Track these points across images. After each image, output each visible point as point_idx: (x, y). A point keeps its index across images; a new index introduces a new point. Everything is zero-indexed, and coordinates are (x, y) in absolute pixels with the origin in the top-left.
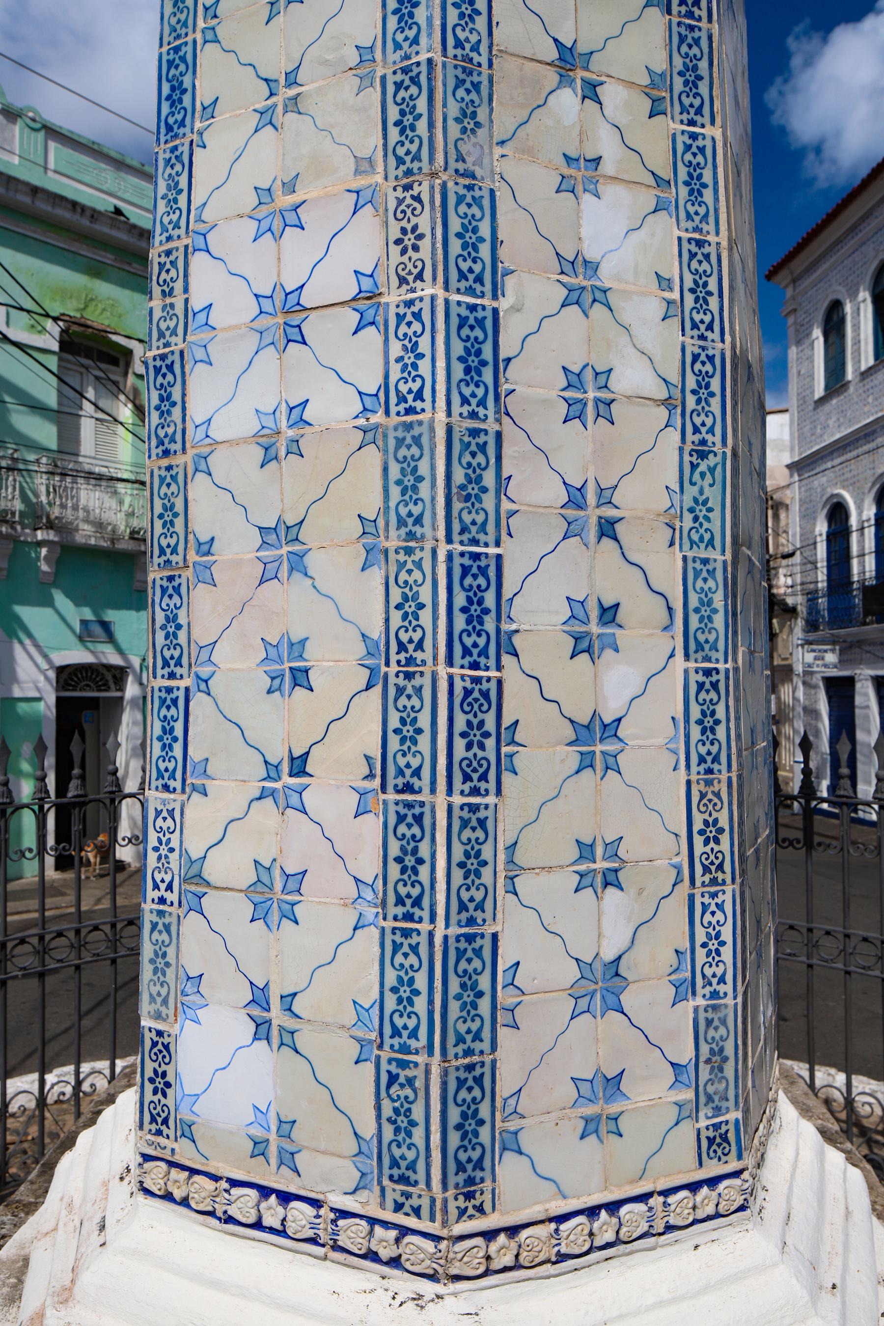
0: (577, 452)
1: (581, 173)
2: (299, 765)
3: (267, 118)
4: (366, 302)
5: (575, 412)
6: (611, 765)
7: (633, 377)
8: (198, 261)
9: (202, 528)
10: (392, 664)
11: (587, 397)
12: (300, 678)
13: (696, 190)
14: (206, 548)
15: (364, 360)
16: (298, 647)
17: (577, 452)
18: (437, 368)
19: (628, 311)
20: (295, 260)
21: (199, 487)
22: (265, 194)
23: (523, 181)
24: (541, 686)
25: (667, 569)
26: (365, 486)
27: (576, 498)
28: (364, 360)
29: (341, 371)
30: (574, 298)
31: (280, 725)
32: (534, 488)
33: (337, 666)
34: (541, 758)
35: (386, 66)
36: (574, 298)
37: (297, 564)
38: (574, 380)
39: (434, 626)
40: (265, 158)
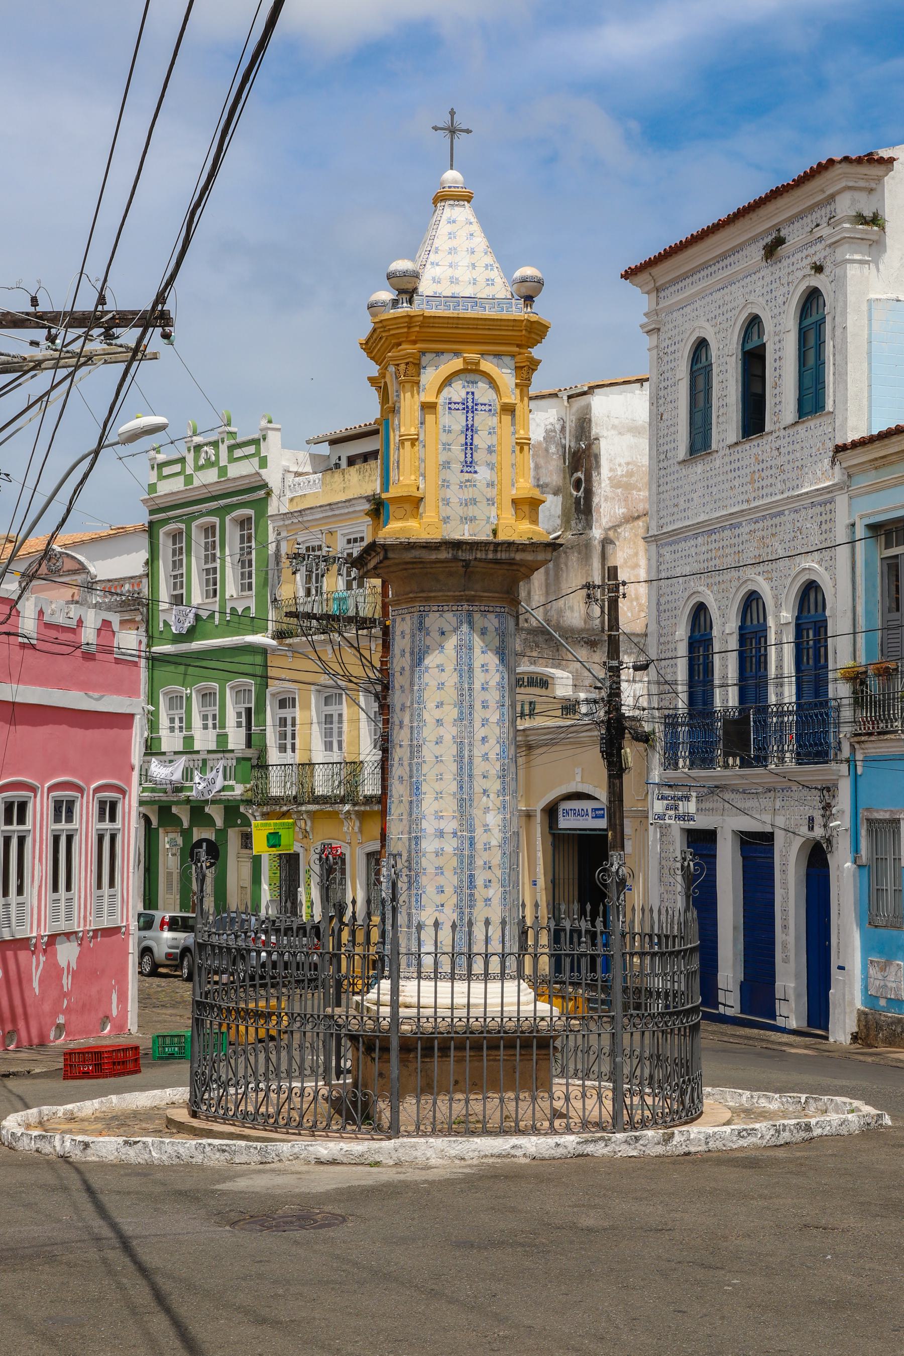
0: (485, 856)
1: (487, 810)
2: (442, 905)
3: (436, 798)
4: (455, 834)
5: (485, 849)
6: (490, 905)
7: (494, 843)
8: (423, 821)
9: (424, 865)
10: (458, 890)
11: (487, 847)
12: (442, 892)
13: (504, 808)
14: (425, 869)
15: (454, 843)
16: (442, 887)
17: (485, 856)
18: (466, 845)
19: (493, 832)
20: (443, 825)
21: (423, 859)
22: (436, 812)
23: (477, 812)
24: (480, 892)
25: (499, 873)
26: (454, 862)
27: (485, 863)
28: (454, 843)
29: (450, 845)
30: (485, 831)
31: (439, 899)
32: (479, 862)
33: (449, 890)
34: (480, 904)
35: (458, 796)
36: (485, 831)
37: (442, 873)
38: (485, 845)
39: (465, 884)
40: (436, 806)
